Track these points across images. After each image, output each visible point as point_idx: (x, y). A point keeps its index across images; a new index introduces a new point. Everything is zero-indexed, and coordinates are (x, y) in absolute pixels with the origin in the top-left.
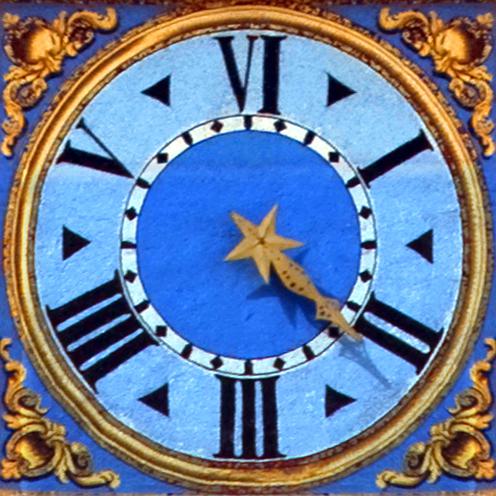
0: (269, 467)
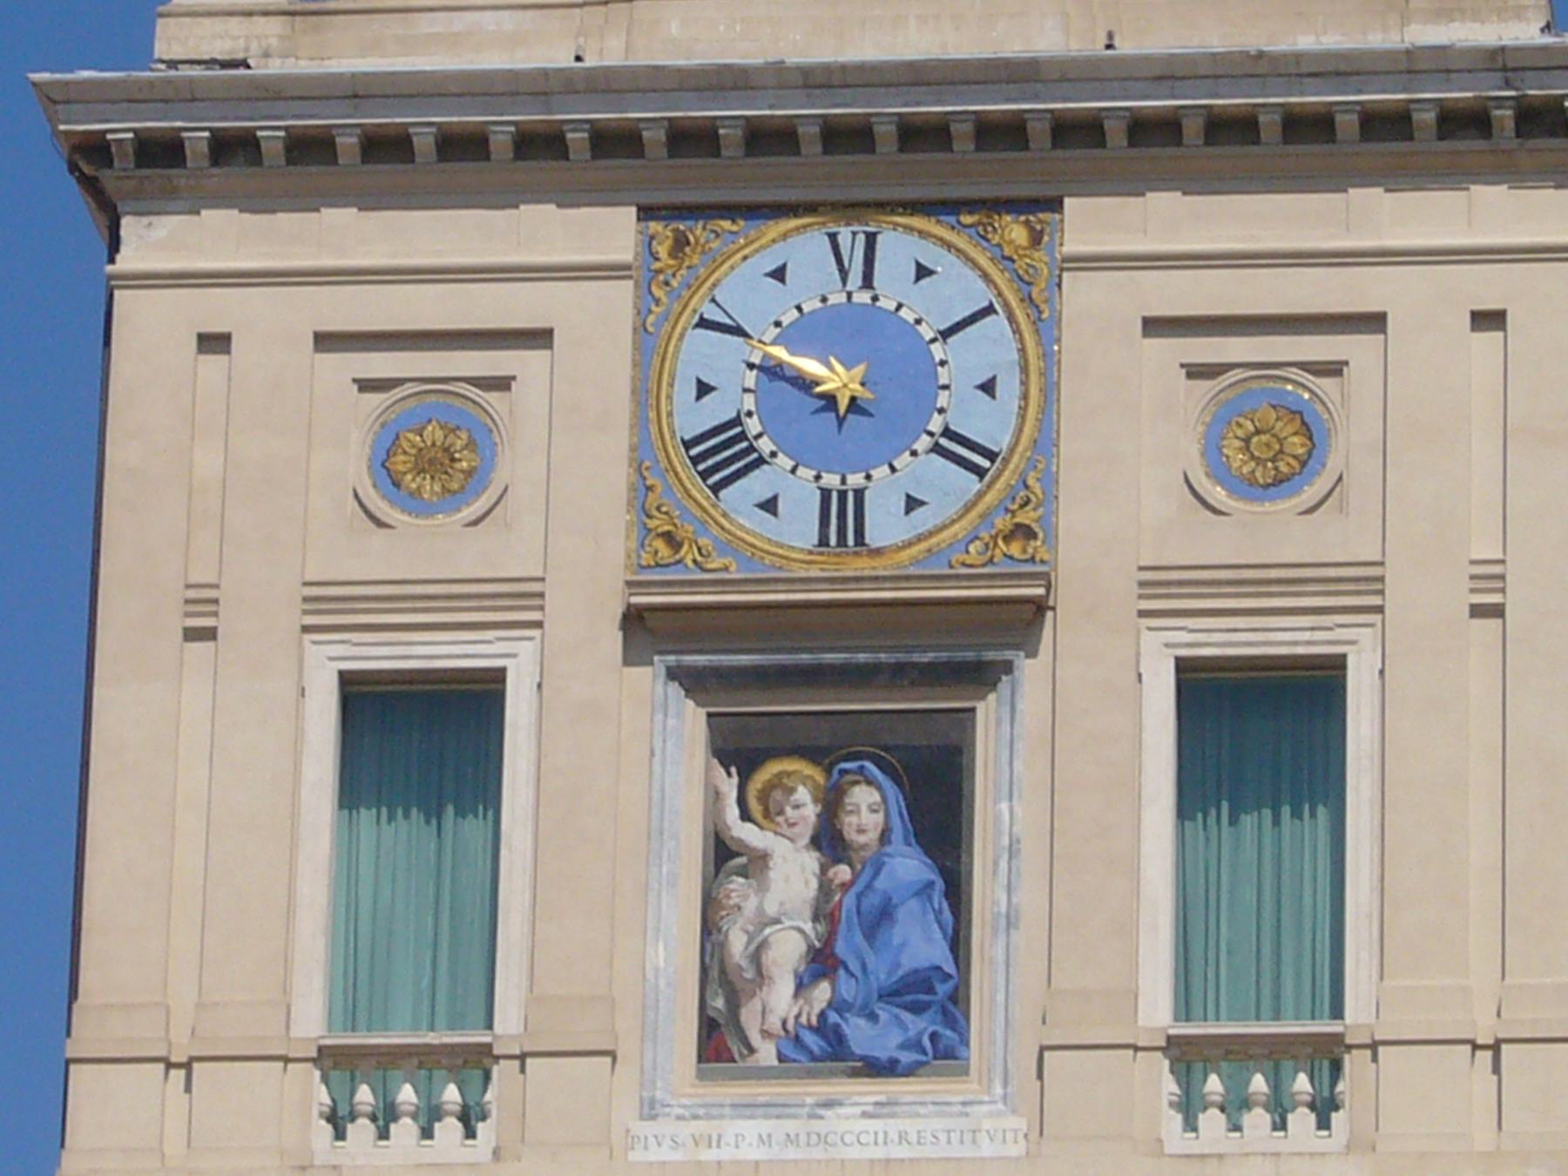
0: (856, 553)
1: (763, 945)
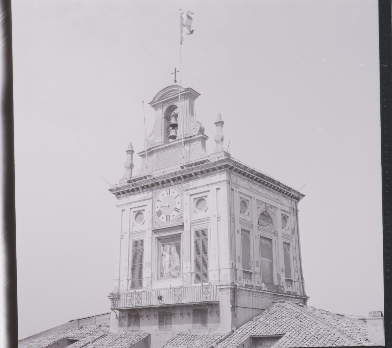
1: (165, 264)
